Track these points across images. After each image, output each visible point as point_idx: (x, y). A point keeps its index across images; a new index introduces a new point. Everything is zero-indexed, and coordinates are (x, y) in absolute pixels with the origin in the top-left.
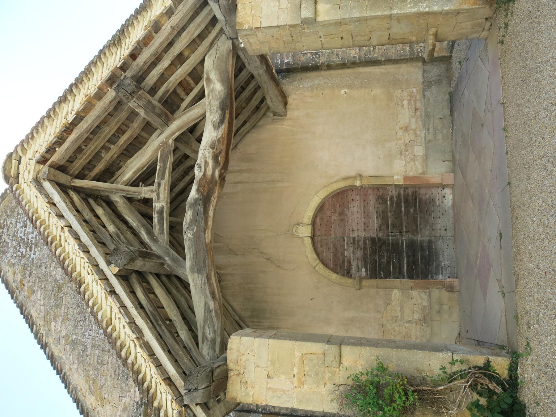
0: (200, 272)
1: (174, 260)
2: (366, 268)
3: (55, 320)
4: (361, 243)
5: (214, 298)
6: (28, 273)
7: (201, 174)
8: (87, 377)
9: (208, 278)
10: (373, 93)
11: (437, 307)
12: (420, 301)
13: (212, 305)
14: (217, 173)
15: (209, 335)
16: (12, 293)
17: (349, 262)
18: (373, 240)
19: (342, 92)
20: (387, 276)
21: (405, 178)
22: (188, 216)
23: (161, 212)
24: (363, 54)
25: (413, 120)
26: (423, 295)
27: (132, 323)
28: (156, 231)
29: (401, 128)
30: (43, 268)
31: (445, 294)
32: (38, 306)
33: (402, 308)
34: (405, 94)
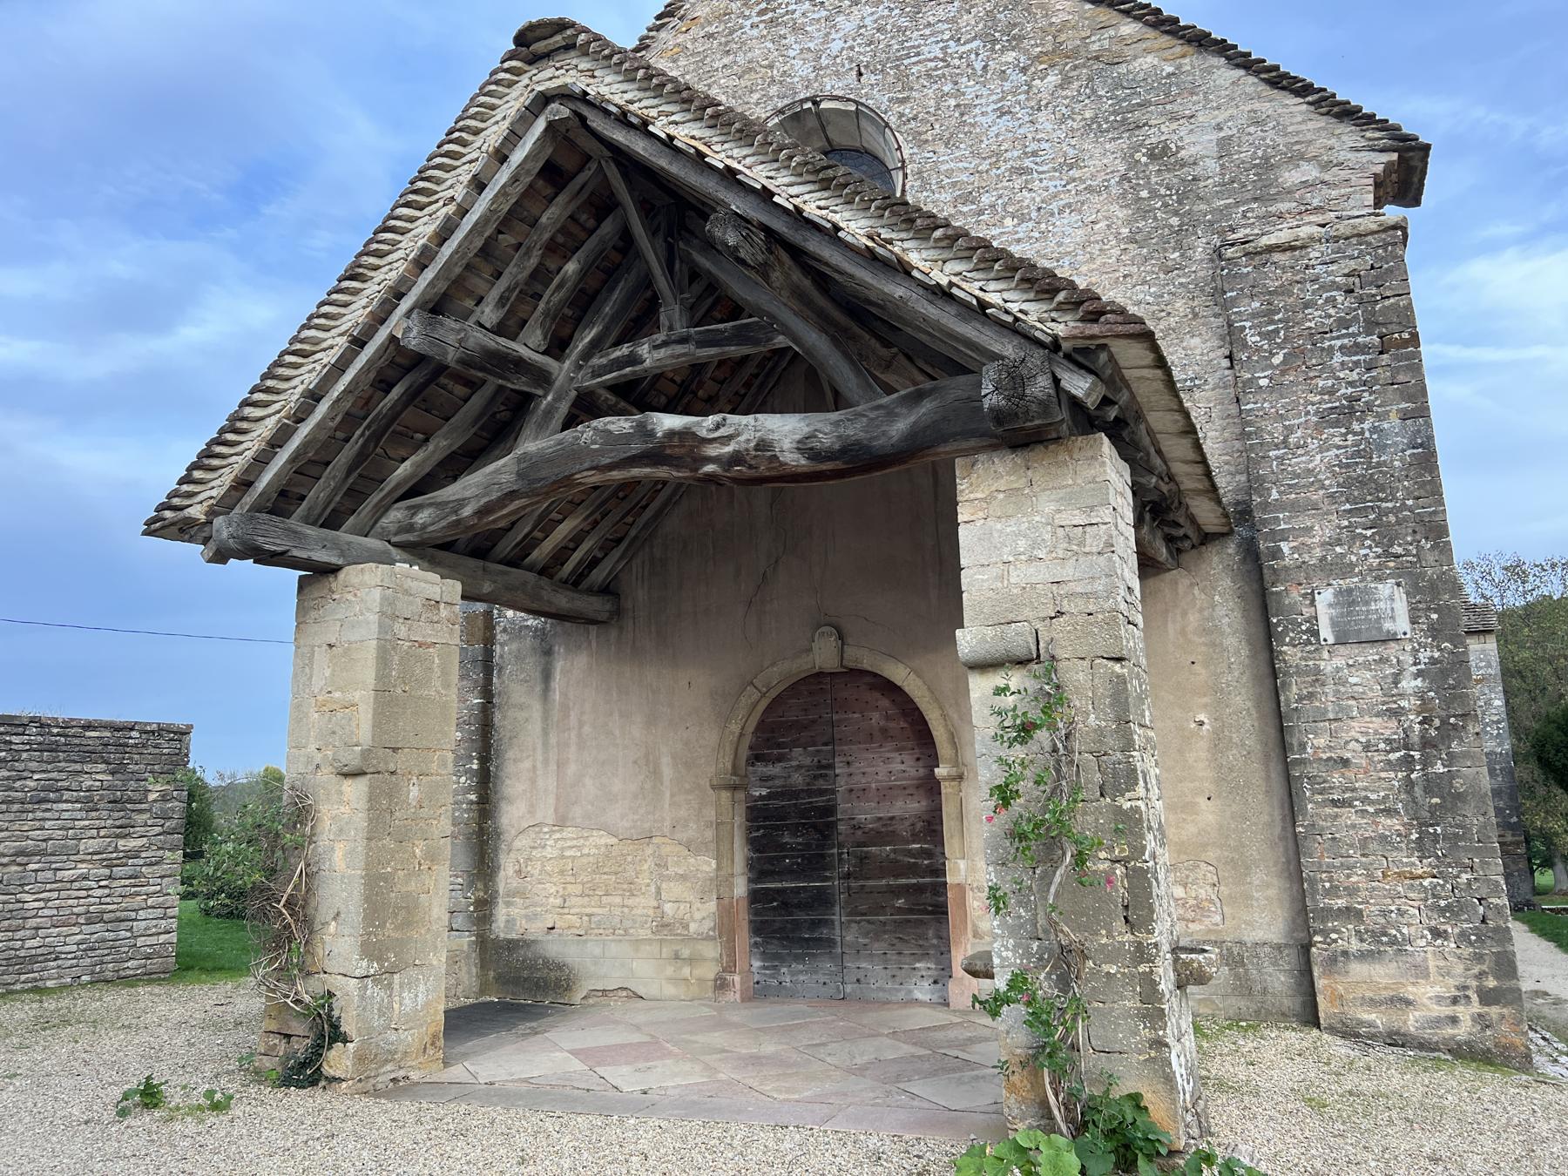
1: (549, 412)
2: (769, 796)
4: (821, 784)
5: (482, 512)
7: (703, 433)
9: (512, 495)
10: (1202, 801)
11: (686, 953)
12: (698, 916)
13: (467, 511)
14: (710, 468)
15: (422, 518)
17: (780, 759)
18: (830, 810)
19: (1201, 717)
20: (754, 844)
21: (961, 888)
22: (620, 425)
23: (633, 359)
24: (1312, 770)
26: (709, 924)
27: (314, 396)
28: (596, 361)
30: (726, 61)
31: (709, 971)
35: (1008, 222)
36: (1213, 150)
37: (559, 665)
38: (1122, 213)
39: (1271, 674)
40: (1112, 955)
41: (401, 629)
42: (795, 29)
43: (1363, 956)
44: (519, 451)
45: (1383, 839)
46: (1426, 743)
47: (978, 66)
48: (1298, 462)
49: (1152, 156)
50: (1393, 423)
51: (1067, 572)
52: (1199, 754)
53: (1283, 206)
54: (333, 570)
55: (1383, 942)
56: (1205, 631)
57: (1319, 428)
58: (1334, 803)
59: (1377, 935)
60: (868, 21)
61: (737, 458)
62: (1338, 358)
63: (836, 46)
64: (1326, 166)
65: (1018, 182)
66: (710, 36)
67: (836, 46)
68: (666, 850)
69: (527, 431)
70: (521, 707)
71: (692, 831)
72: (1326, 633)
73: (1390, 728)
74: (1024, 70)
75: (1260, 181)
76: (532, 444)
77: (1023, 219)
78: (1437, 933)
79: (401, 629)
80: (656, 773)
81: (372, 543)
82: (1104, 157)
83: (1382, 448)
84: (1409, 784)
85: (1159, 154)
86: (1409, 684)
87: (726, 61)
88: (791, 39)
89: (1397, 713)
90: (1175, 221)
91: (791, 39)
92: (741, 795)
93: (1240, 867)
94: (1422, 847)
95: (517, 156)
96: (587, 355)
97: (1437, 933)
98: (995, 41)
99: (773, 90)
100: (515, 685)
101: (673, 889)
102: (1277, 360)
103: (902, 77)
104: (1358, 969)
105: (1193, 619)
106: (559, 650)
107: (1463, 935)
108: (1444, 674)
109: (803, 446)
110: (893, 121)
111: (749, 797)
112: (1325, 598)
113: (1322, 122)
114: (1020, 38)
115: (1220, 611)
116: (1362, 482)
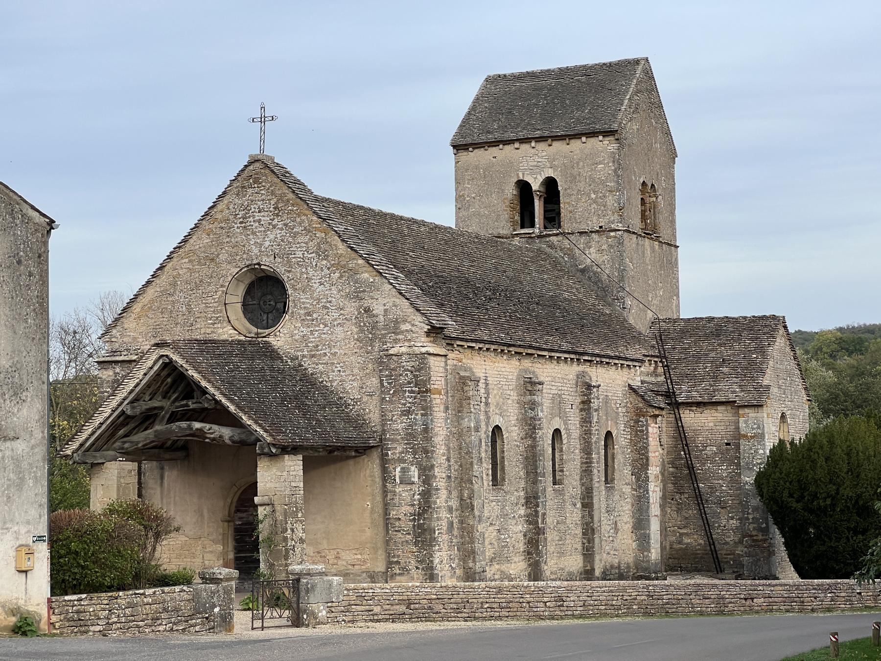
0: (155, 436)
2: (242, 524)
3: (190, 261)
5: (144, 446)
6: (223, 225)
8: (152, 301)
9: (153, 442)
13: (140, 445)
14: (207, 440)
16: (206, 214)
17: (246, 511)
20: (237, 541)
22: (184, 424)
25: (344, 563)
28: (177, 404)
29: (338, 553)
30: (228, 240)
32: (201, 241)
33: (211, 552)
34: (366, 557)
35: (322, 326)
36: (383, 313)
37: (166, 474)
38: (355, 330)
39: (385, 492)
40: (281, 565)
41: (122, 481)
42: (254, 233)
43: (400, 574)
44: (154, 429)
45: (407, 541)
46: (419, 514)
47: (314, 264)
48: (395, 426)
49: (365, 311)
50: (419, 417)
51: (277, 485)
52: (367, 514)
53: (401, 337)
54: (103, 463)
55: (405, 571)
56: (371, 476)
57: (401, 416)
58: (396, 531)
59: (403, 568)
60: (278, 236)
61: (214, 439)
62: (407, 394)
63: (267, 244)
64: (413, 325)
65: (325, 312)
66: (222, 228)
67: (267, 244)
68: (205, 542)
69: (157, 422)
70: (152, 489)
71: (214, 537)
72: (398, 480)
73: (411, 510)
74: (329, 269)
75: (394, 326)
76: (158, 427)
77: (326, 326)
78: (417, 568)
79: (122, 481)
80: (202, 515)
81: (111, 453)
82: (351, 308)
83: (416, 424)
84: (414, 525)
85: (367, 310)
86: (417, 497)
87: (228, 240)
88: (251, 237)
89: (413, 505)
90: (370, 336)
91: (251, 237)
92: (232, 524)
93: (375, 549)
94: (416, 544)
95: (156, 368)
96: (174, 402)
97: (417, 568)
98: (320, 256)
99: (245, 256)
100: (151, 481)
101: (208, 556)
102: (391, 392)
103: (289, 262)
104: (398, 578)
105: (368, 471)
106: (166, 468)
107: (423, 569)
108: (425, 494)
109: (230, 438)
110: (286, 279)
111: (235, 525)
112: (398, 469)
113: (412, 310)
114: (328, 256)
115: (375, 470)
116: (410, 434)
